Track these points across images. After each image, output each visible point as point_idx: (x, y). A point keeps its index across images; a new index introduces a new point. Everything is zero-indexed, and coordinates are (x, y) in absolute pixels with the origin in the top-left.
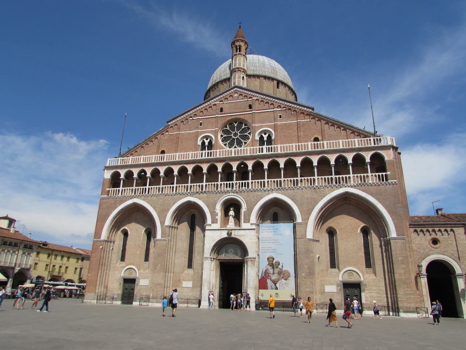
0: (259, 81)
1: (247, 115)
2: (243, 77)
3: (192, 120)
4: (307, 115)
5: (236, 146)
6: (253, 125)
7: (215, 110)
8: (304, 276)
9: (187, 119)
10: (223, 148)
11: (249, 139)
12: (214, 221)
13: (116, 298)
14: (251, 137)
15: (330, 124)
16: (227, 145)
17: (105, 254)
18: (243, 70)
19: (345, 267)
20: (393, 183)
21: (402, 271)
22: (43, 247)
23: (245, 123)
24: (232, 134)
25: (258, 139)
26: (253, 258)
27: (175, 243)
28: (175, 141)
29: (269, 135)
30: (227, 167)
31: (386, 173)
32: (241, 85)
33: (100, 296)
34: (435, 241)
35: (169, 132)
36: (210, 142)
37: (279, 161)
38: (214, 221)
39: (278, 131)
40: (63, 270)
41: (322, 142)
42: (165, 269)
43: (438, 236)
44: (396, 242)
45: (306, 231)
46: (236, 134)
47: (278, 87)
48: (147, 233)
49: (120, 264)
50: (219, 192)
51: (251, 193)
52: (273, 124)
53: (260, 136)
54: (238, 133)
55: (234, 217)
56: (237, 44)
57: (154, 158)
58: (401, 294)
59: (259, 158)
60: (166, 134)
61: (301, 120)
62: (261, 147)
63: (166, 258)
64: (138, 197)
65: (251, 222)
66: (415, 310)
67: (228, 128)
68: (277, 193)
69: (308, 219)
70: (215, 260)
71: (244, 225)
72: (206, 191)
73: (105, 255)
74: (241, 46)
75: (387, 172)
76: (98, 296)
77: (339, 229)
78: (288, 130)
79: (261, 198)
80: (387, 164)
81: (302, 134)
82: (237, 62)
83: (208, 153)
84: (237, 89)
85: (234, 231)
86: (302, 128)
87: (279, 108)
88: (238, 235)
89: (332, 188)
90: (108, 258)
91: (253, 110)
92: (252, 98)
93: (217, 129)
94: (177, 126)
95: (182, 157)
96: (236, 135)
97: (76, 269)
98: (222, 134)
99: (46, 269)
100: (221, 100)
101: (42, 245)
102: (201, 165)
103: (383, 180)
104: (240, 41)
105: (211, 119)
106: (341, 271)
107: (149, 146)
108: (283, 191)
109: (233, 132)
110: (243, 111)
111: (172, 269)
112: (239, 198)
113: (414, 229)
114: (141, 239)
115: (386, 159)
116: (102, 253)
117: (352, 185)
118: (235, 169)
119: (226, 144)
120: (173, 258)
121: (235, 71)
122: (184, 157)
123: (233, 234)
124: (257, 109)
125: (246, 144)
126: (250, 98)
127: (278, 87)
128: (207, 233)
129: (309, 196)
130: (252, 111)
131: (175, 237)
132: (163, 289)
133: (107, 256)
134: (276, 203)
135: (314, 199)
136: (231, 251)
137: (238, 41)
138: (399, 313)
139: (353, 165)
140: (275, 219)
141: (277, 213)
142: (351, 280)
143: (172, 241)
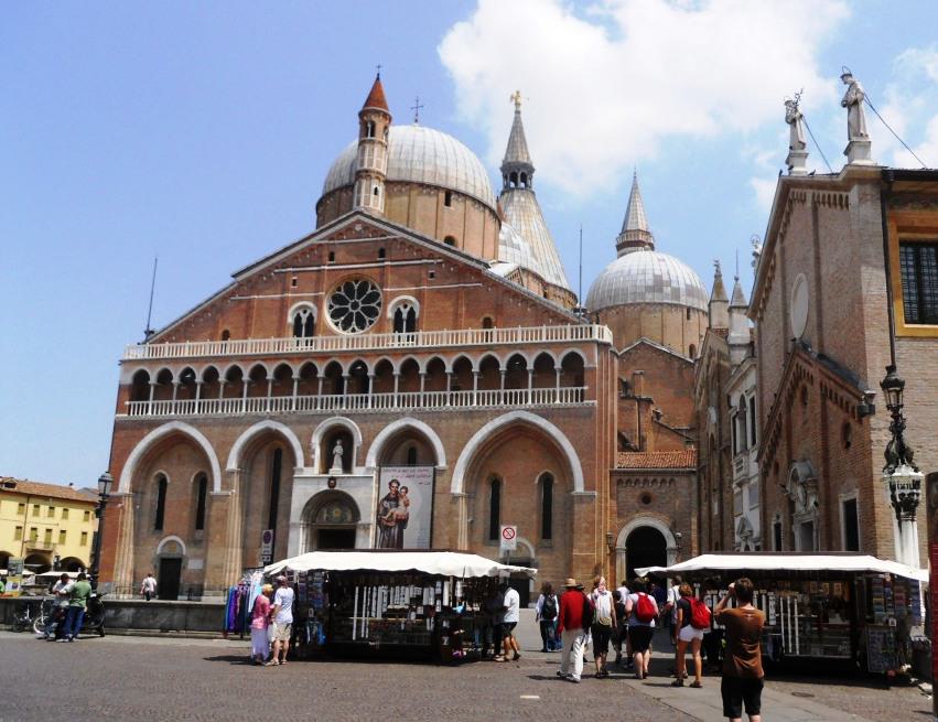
2: (376, 189)
14: (380, 312)
22: (7, 489)
30: (334, 369)
36: (311, 318)
38: (309, 463)
40: (55, 538)
45: (450, 482)
46: (356, 306)
49: (153, 533)
65: (367, 465)
82: (366, 158)
96: (355, 306)
99: (18, 537)
103: (577, 400)
112: (351, 424)
114: (190, 491)
118: (345, 373)
121: (361, 177)
127: (448, 203)
130: (383, 261)
134: (409, 433)
140: (411, 460)
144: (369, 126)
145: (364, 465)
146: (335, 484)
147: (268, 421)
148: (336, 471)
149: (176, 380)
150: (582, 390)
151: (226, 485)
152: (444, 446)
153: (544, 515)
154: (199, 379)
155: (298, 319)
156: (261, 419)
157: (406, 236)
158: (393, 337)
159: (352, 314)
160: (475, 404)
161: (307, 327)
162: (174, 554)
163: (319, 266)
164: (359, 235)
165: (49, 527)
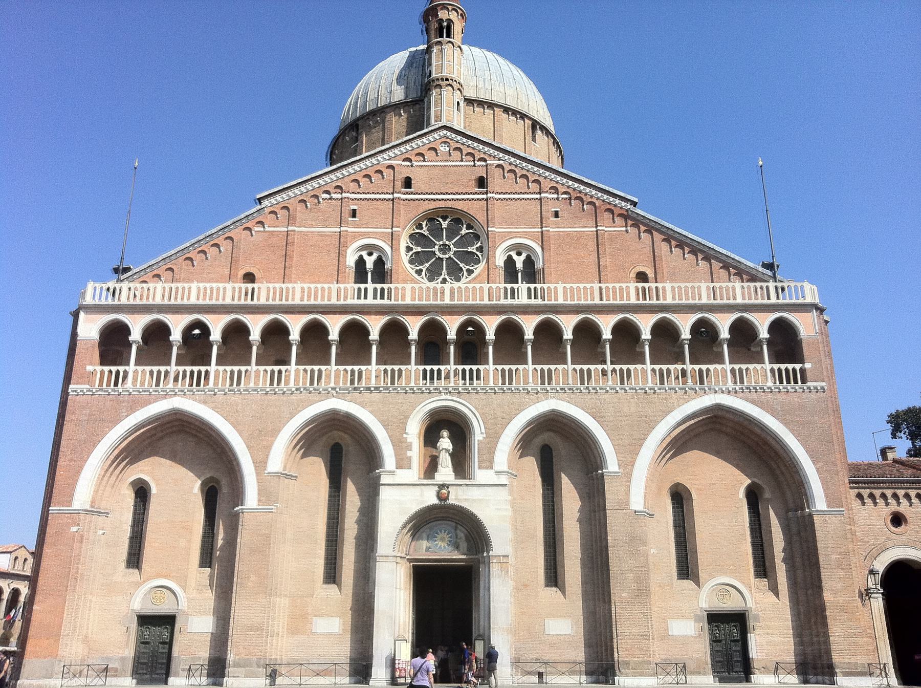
1: (473, 202)
2: (458, 102)
3: (330, 201)
4: (620, 215)
5: (447, 277)
8: (627, 598)
9: (316, 197)
10: (414, 281)
12: (403, 463)
15: (674, 243)
16: (423, 273)
19: (712, 576)
21: (839, 585)
23: (468, 222)
24: (437, 247)
25: (503, 266)
26: (503, 556)
29: (528, 257)
31: (801, 365)
34: (898, 520)
35: (266, 226)
36: (380, 263)
37: (561, 323)
41: (653, 285)
43: (904, 508)
45: (628, 493)
48: (205, 491)
50: (412, 389)
51: (493, 396)
52: (538, 232)
55: (451, 455)
56: (443, 14)
58: (837, 634)
59: (511, 312)
61: (606, 227)
62: (509, 286)
64: (184, 395)
65: (497, 467)
66: (866, 670)
68: (558, 399)
69: (633, 464)
72: (380, 387)
74: (453, 22)
75: (803, 363)
77: (698, 489)
78: (575, 248)
79: (520, 411)
80: (804, 345)
81: (608, 260)
83: (375, 290)
86: (607, 246)
87: (553, 193)
89: (686, 392)
92: (485, 161)
93: (397, 232)
94: (289, 212)
95: (304, 295)
96: (445, 249)
98: (411, 246)
100: (407, 156)
102: (363, 320)
105: (380, 202)
107: (207, 259)
108: (572, 395)
117: (730, 389)
118: (452, 335)
119: (421, 270)
121: (440, 86)
122: (311, 294)
124: (500, 191)
125: (473, 276)
126: (481, 160)
127: (534, 139)
128: (385, 495)
129: (633, 409)
130: (487, 193)
135: (646, 417)
136: (442, 539)
138: (835, 678)
139: (730, 343)
141: (550, 447)
142: (724, 605)
145: (490, 466)
146: (449, 492)
149: (176, 336)
150: (803, 371)
151: (265, 494)
159: (442, 259)
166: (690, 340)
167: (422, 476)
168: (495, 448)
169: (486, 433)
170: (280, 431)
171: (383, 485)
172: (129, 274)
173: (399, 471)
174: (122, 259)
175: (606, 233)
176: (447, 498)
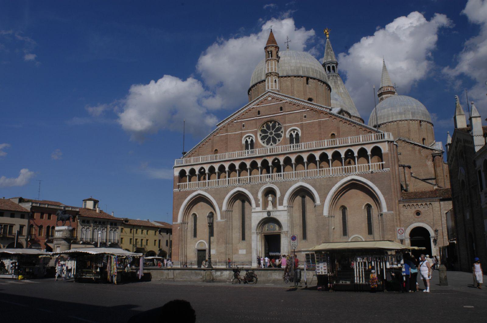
0: (290, 81)
2: (275, 80)
6: (284, 125)
7: (254, 113)
11: (281, 136)
13: (194, 264)
14: (283, 135)
16: (265, 143)
17: (182, 233)
18: (275, 74)
19: (353, 235)
20: (387, 170)
22: (126, 223)
24: (269, 133)
27: (231, 223)
28: (225, 142)
29: (297, 133)
30: (265, 163)
32: (274, 88)
33: (183, 262)
34: (418, 213)
36: (252, 141)
39: (304, 129)
40: (144, 243)
42: (225, 242)
43: (421, 209)
44: (387, 216)
45: (323, 210)
46: (271, 133)
47: (307, 83)
53: (290, 134)
54: (273, 132)
55: (272, 202)
57: (209, 158)
60: (217, 135)
63: (225, 234)
67: (265, 128)
69: (324, 201)
70: (260, 234)
71: (280, 208)
73: (182, 234)
76: (181, 263)
82: (270, 67)
84: (270, 94)
85: (272, 212)
88: (275, 215)
90: (185, 236)
91: (284, 112)
96: (271, 133)
97: (155, 241)
98: (261, 134)
99: (130, 243)
100: (258, 104)
101: (124, 222)
103: (380, 169)
104: (271, 46)
106: (350, 237)
109: (269, 131)
110: (276, 113)
111: (231, 241)
112: (275, 187)
113: (403, 204)
115: (383, 151)
116: (180, 232)
118: (270, 164)
120: (231, 234)
121: (268, 76)
123: (271, 215)
124: (287, 111)
125: (280, 141)
127: (307, 83)
128: (253, 215)
131: (231, 218)
132: (225, 256)
133: (184, 234)
137: (269, 46)
143: (229, 221)
144: (270, 52)
146: (270, 214)
147: (238, 188)
148: (270, 208)
150: (382, 164)
152: (318, 194)
153: (368, 224)
154: (207, 171)
155: (247, 142)
156: (235, 187)
157: (292, 100)
158: (290, 146)
160: (331, 174)
161: (251, 145)
162: (203, 248)
163: (254, 117)
164: (270, 102)
165: (142, 238)
166: (344, 158)
167: (264, 209)
168: (283, 199)
169: (281, 194)
170: (225, 198)
171: (253, 212)
172: (186, 154)
173: (256, 208)
174: (184, 150)
175: (321, 121)
176: (270, 215)
